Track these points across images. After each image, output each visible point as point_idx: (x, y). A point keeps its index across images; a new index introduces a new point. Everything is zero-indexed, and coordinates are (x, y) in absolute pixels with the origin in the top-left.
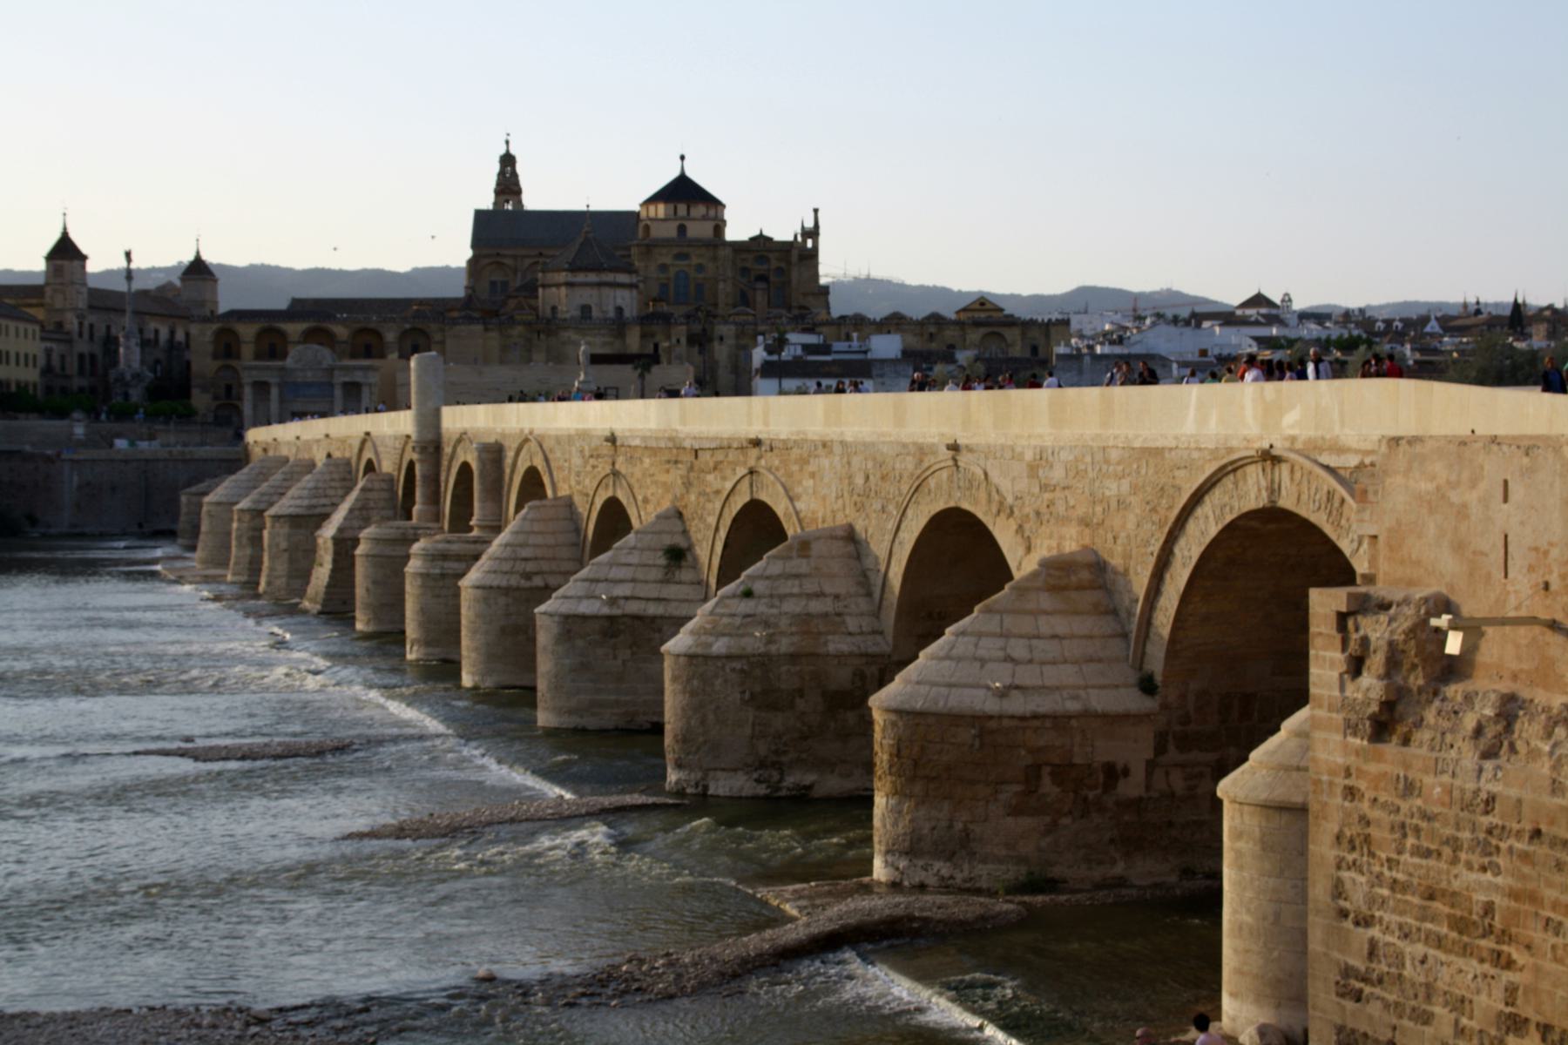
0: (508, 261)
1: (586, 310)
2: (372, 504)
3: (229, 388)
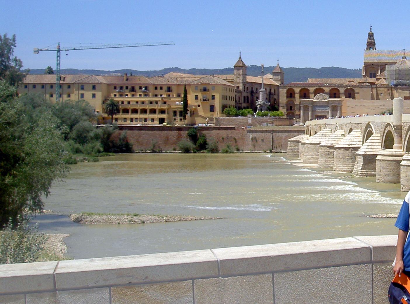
2: (374, 144)
3: (291, 107)
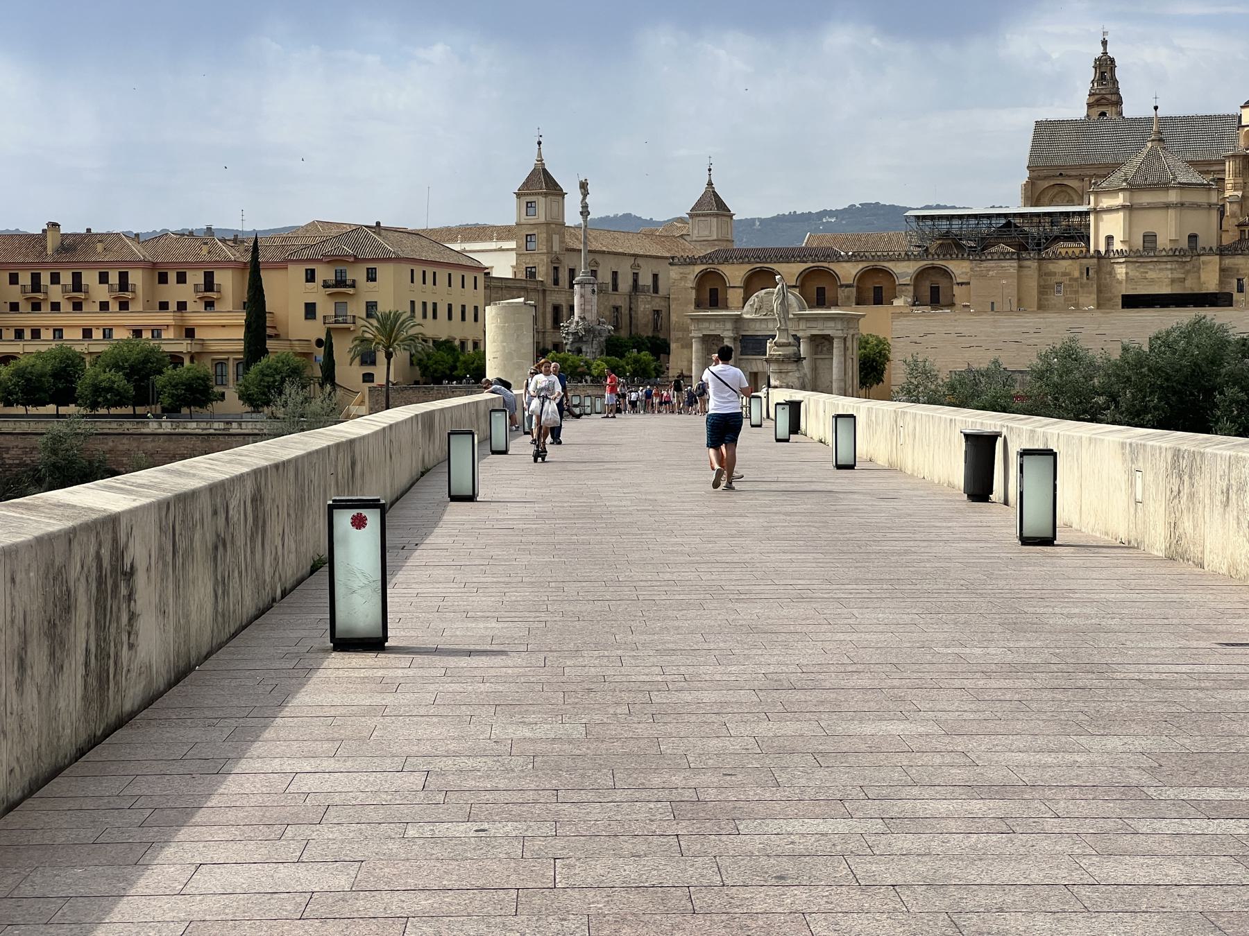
0: (1074, 183)
1: (1150, 238)
